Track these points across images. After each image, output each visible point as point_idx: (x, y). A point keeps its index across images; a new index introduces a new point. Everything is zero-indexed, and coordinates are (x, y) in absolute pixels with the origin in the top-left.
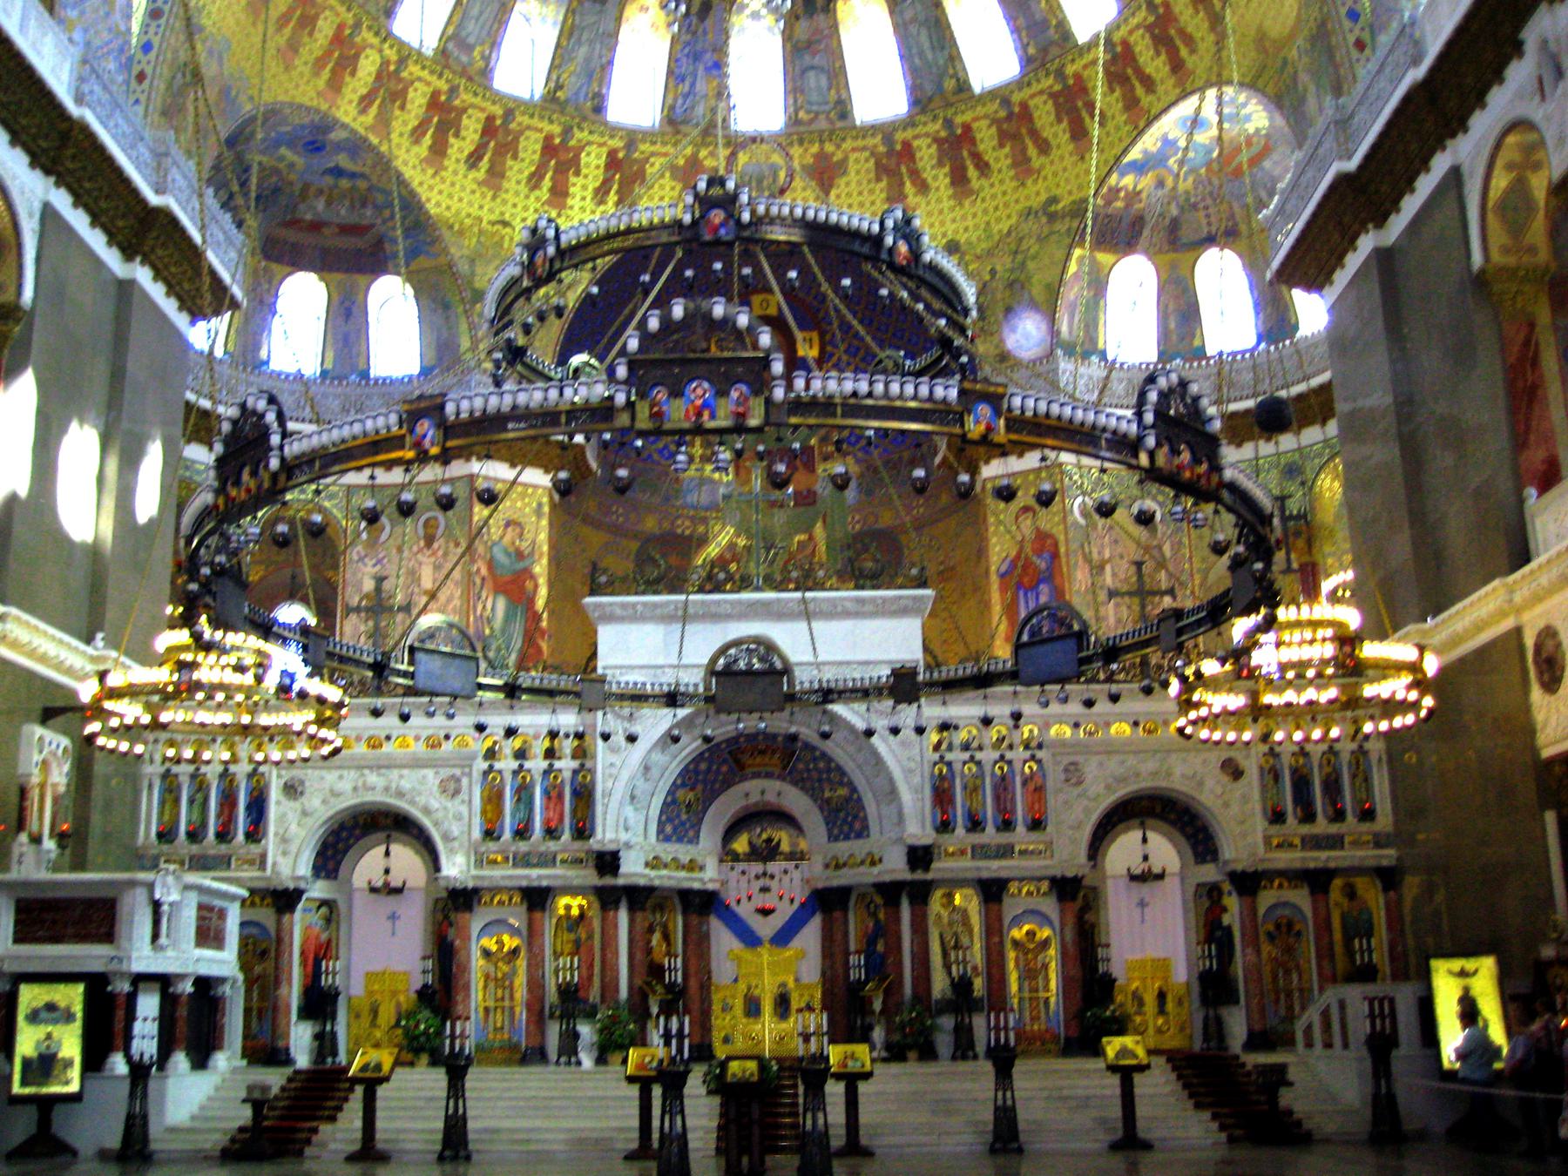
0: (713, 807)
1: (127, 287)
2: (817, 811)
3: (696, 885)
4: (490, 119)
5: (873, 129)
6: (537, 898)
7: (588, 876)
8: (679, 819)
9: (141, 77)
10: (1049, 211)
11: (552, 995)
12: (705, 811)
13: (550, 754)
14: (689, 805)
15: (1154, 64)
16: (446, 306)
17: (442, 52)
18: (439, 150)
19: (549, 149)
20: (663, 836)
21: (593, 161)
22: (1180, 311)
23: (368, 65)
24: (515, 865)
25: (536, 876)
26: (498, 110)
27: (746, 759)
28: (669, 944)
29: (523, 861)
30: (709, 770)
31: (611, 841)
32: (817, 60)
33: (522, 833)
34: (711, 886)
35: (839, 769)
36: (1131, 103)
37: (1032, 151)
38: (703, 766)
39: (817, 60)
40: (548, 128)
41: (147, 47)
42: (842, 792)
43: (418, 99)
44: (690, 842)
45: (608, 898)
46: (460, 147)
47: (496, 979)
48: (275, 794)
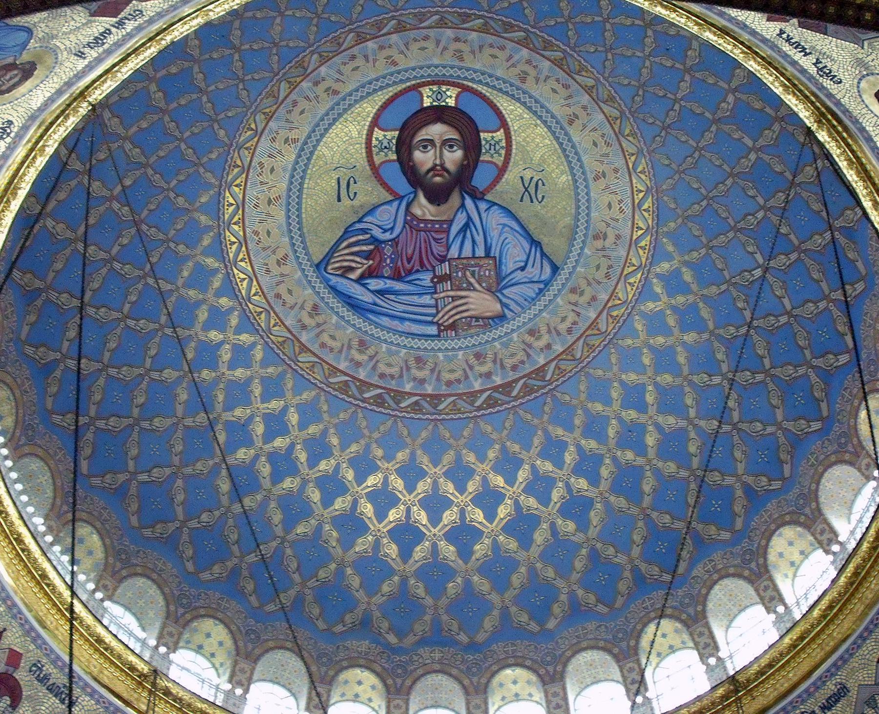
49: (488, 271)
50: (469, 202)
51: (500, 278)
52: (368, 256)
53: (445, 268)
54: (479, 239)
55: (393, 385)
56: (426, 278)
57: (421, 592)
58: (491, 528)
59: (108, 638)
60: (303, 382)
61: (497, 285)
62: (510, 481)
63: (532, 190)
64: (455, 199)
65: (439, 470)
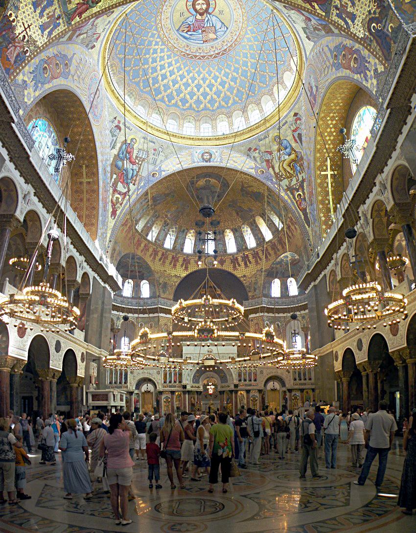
0: (203, 376)
1: (104, 288)
4: (163, 253)
5: (231, 254)
6: (173, 393)
7: (181, 389)
8: (196, 379)
9: (107, 252)
10: (261, 270)
11: (175, 408)
15: (279, 247)
16: (154, 286)
17: (155, 241)
18: (154, 258)
19: (173, 258)
20: (193, 382)
21: (181, 260)
22: (284, 288)
23: (142, 245)
25: (173, 389)
26: (165, 251)
29: (170, 387)
32: (221, 242)
33: (170, 382)
36: (275, 253)
37: (259, 260)
39: (221, 242)
40: (173, 254)
41: (109, 247)
43: (151, 250)
45: (184, 393)
46: (158, 258)
48: (129, 373)
49: (213, 29)
50: (208, 15)
51: (216, 30)
52: (188, 27)
53: (203, 29)
54: (211, 23)
55: (194, 54)
56: (200, 31)
57: (202, 99)
58: (217, 86)
59: (137, 116)
60: (175, 55)
61: (215, 32)
62: (220, 74)
63: (221, 12)
64: (205, 15)
65: (205, 72)
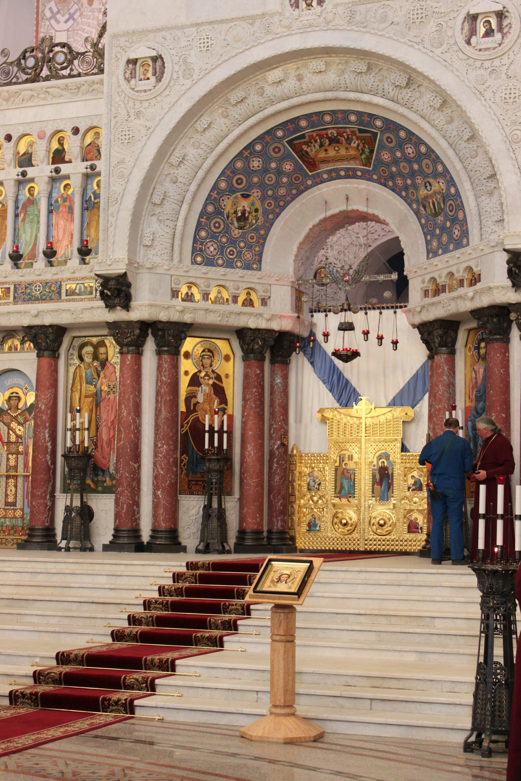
2: (413, 218)
3: (252, 324)
12: (269, 225)
13: (59, 157)
14: (243, 218)
24: (16, 300)
25: (48, 313)
27: (313, 150)
28: (223, 400)
30: (265, 170)
31: (116, 261)
34: (275, 326)
35: (430, 151)
38: (256, 164)
42: (439, 185)
44: (248, 267)
47: (9, 443)
